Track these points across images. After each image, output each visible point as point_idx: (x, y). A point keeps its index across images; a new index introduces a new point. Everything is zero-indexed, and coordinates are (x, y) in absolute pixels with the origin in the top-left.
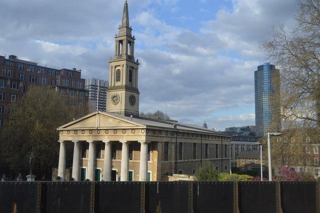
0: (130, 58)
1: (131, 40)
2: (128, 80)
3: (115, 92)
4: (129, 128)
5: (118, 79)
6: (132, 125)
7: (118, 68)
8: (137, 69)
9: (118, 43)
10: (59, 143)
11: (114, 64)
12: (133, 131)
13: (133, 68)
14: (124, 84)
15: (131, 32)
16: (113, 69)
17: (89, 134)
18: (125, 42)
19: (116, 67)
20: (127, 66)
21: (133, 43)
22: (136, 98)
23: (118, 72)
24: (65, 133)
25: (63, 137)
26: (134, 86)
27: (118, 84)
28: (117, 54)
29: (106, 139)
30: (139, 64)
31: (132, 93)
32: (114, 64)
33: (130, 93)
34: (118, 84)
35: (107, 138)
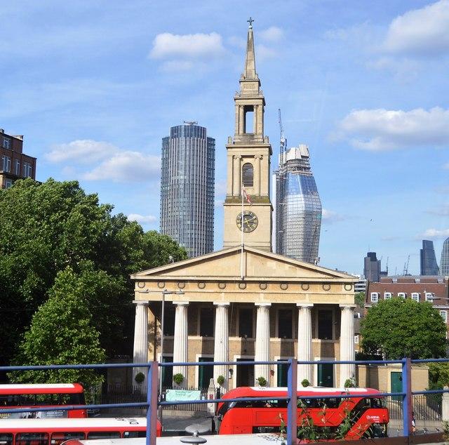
4: (320, 280)
5: (247, 180)
6: (324, 276)
7: (246, 160)
9: (242, 110)
10: (135, 305)
11: (239, 152)
16: (237, 162)
17: (219, 290)
19: (243, 157)
24: (151, 287)
25: (144, 294)
27: (251, 191)
28: (241, 132)
29: (262, 300)
32: (239, 152)
35: (264, 298)
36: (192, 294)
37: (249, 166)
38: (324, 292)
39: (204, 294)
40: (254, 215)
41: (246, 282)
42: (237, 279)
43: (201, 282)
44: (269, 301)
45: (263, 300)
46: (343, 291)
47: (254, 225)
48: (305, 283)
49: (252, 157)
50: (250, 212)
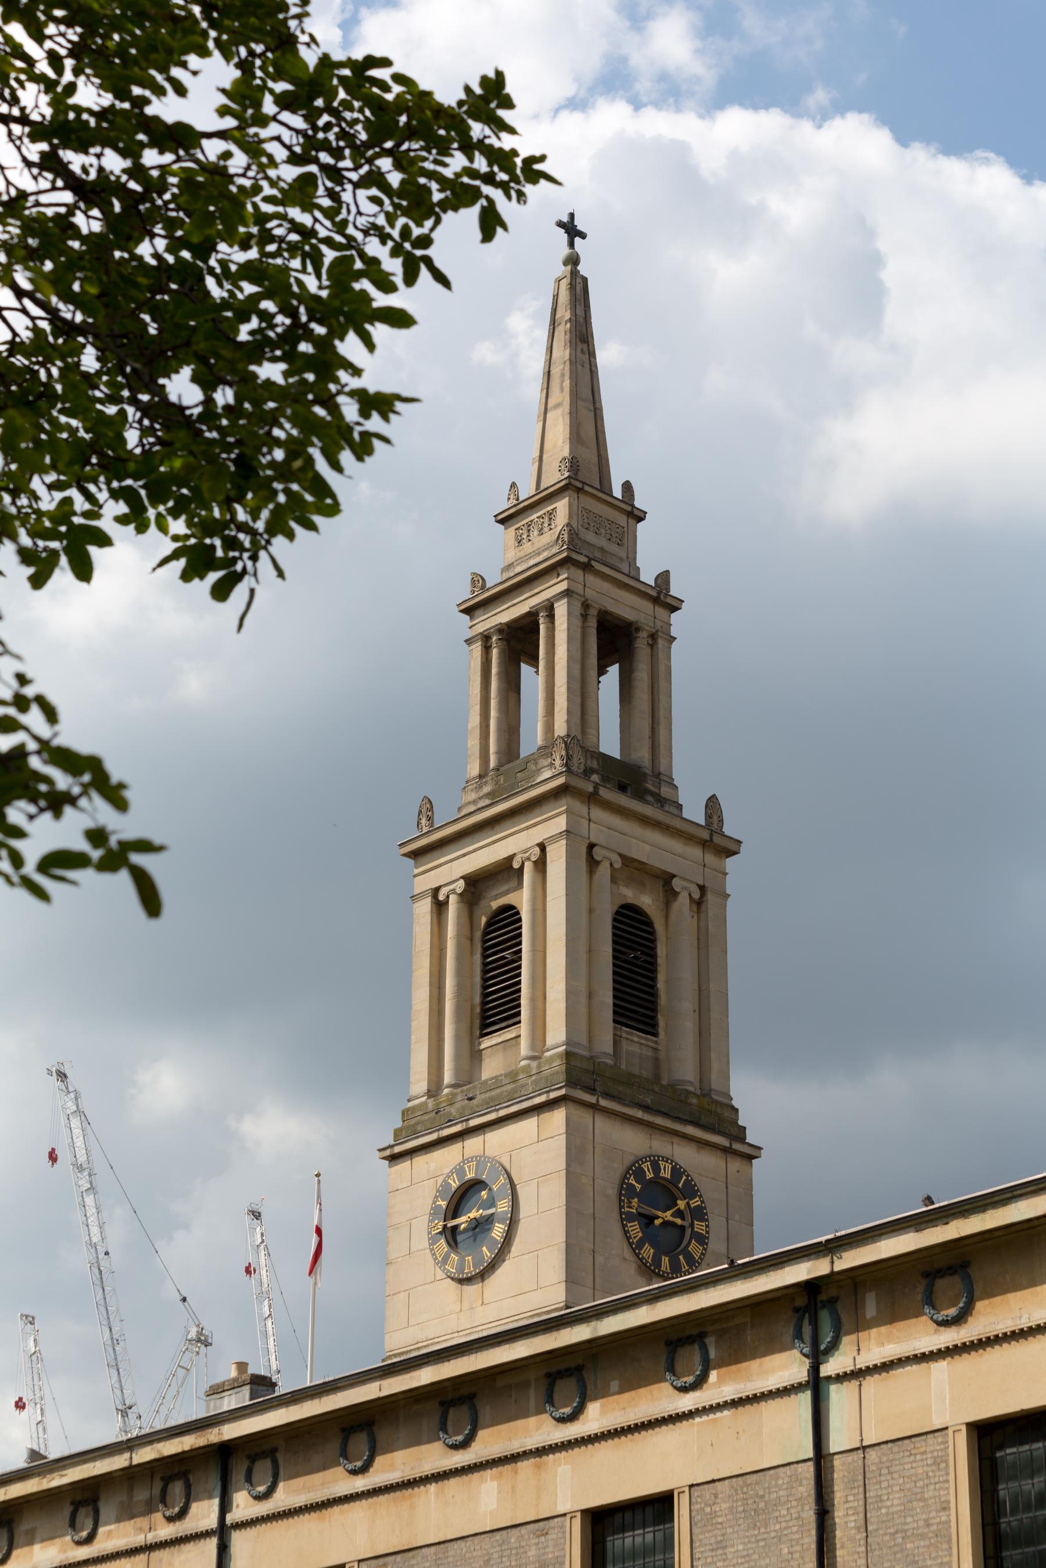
0: (625, 782)
1: (627, 607)
2: (606, 996)
3: (473, 1145)
8: (706, 898)
13: (665, 882)
14: (556, 1034)
15: (627, 541)
18: (560, 640)
19: (476, 885)
20: (588, 858)
21: (660, 638)
22: (711, 1192)
23: (497, 944)
26: (684, 1069)
30: (729, 849)
31: (661, 1146)
32: (452, 870)
33: (633, 1142)
34: (503, 1056)
37: (509, 916)
49: (505, 871)
50: (480, 1160)
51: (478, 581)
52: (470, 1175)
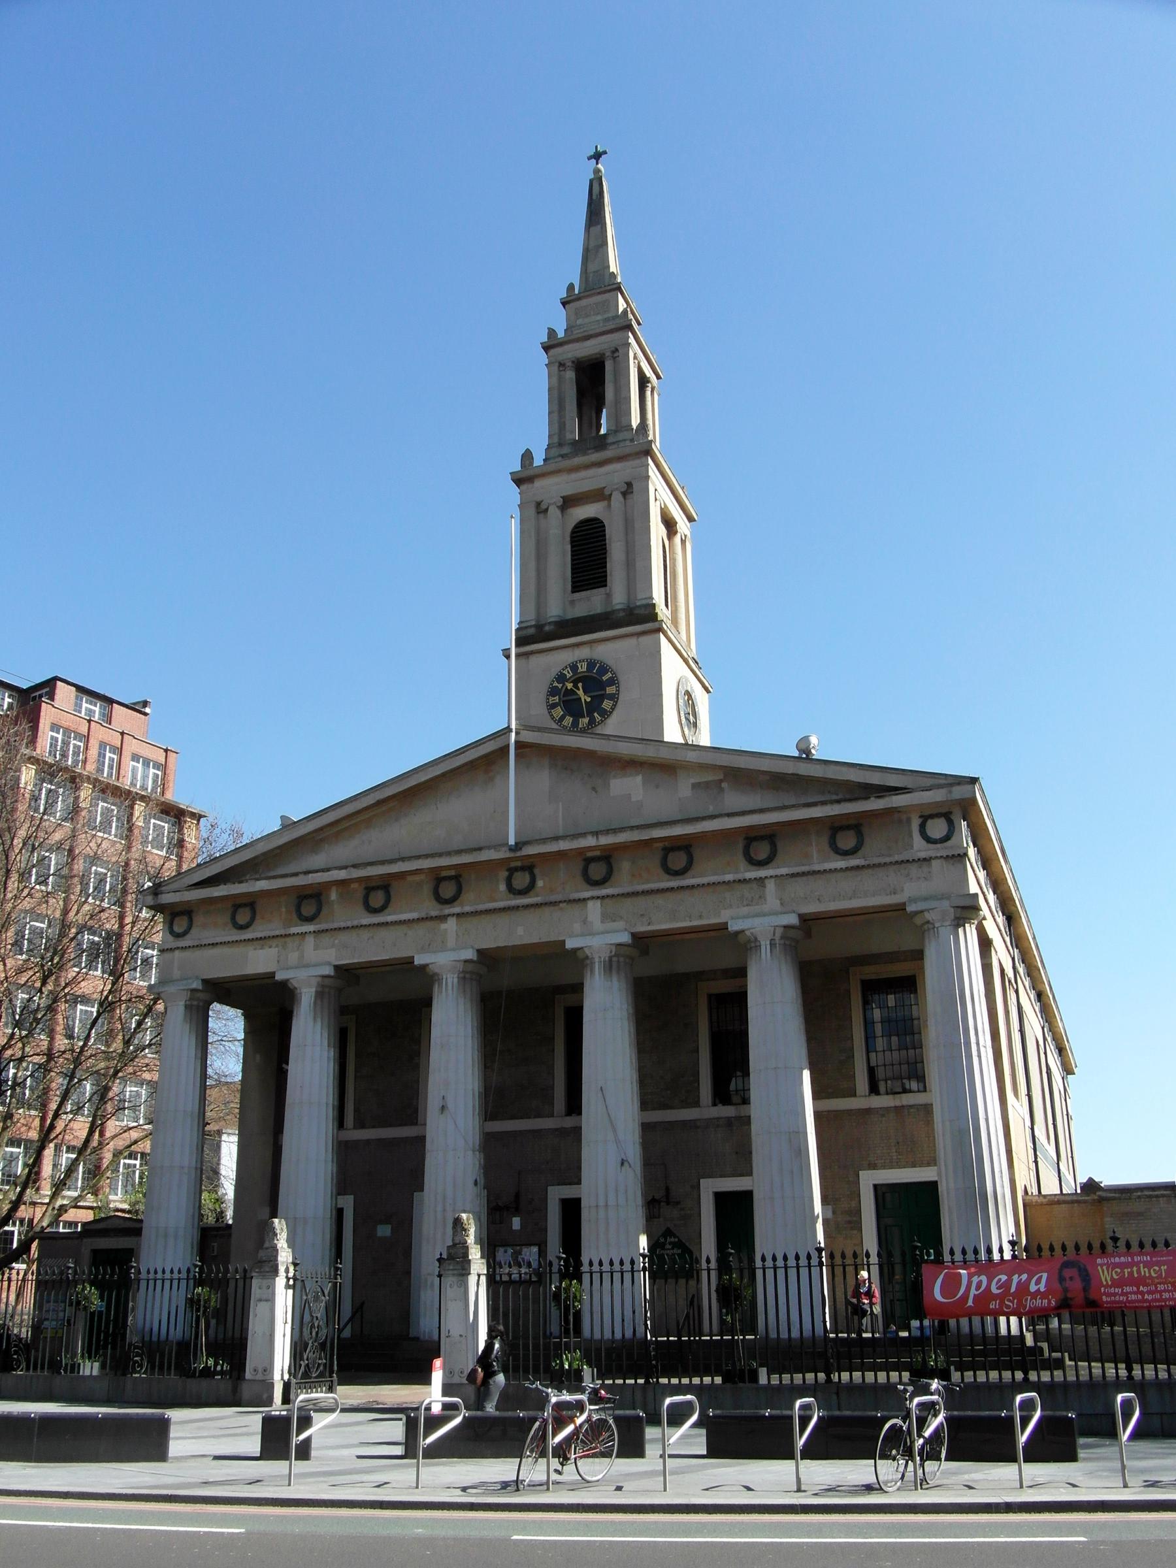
9: (570, 375)
12: (847, 841)
17: (434, 910)
19: (568, 502)
27: (592, 602)
29: (595, 930)
32: (553, 488)
35: (606, 917)
36: (343, 937)
38: (841, 864)
39: (383, 933)
40: (604, 669)
41: (528, 867)
42: (502, 854)
43: (377, 892)
44: (620, 924)
45: (597, 925)
46: (919, 847)
47: (607, 704)
48: (761, 844)
50: (591, 664)
51: (552, 333)
52: (582, 668)
